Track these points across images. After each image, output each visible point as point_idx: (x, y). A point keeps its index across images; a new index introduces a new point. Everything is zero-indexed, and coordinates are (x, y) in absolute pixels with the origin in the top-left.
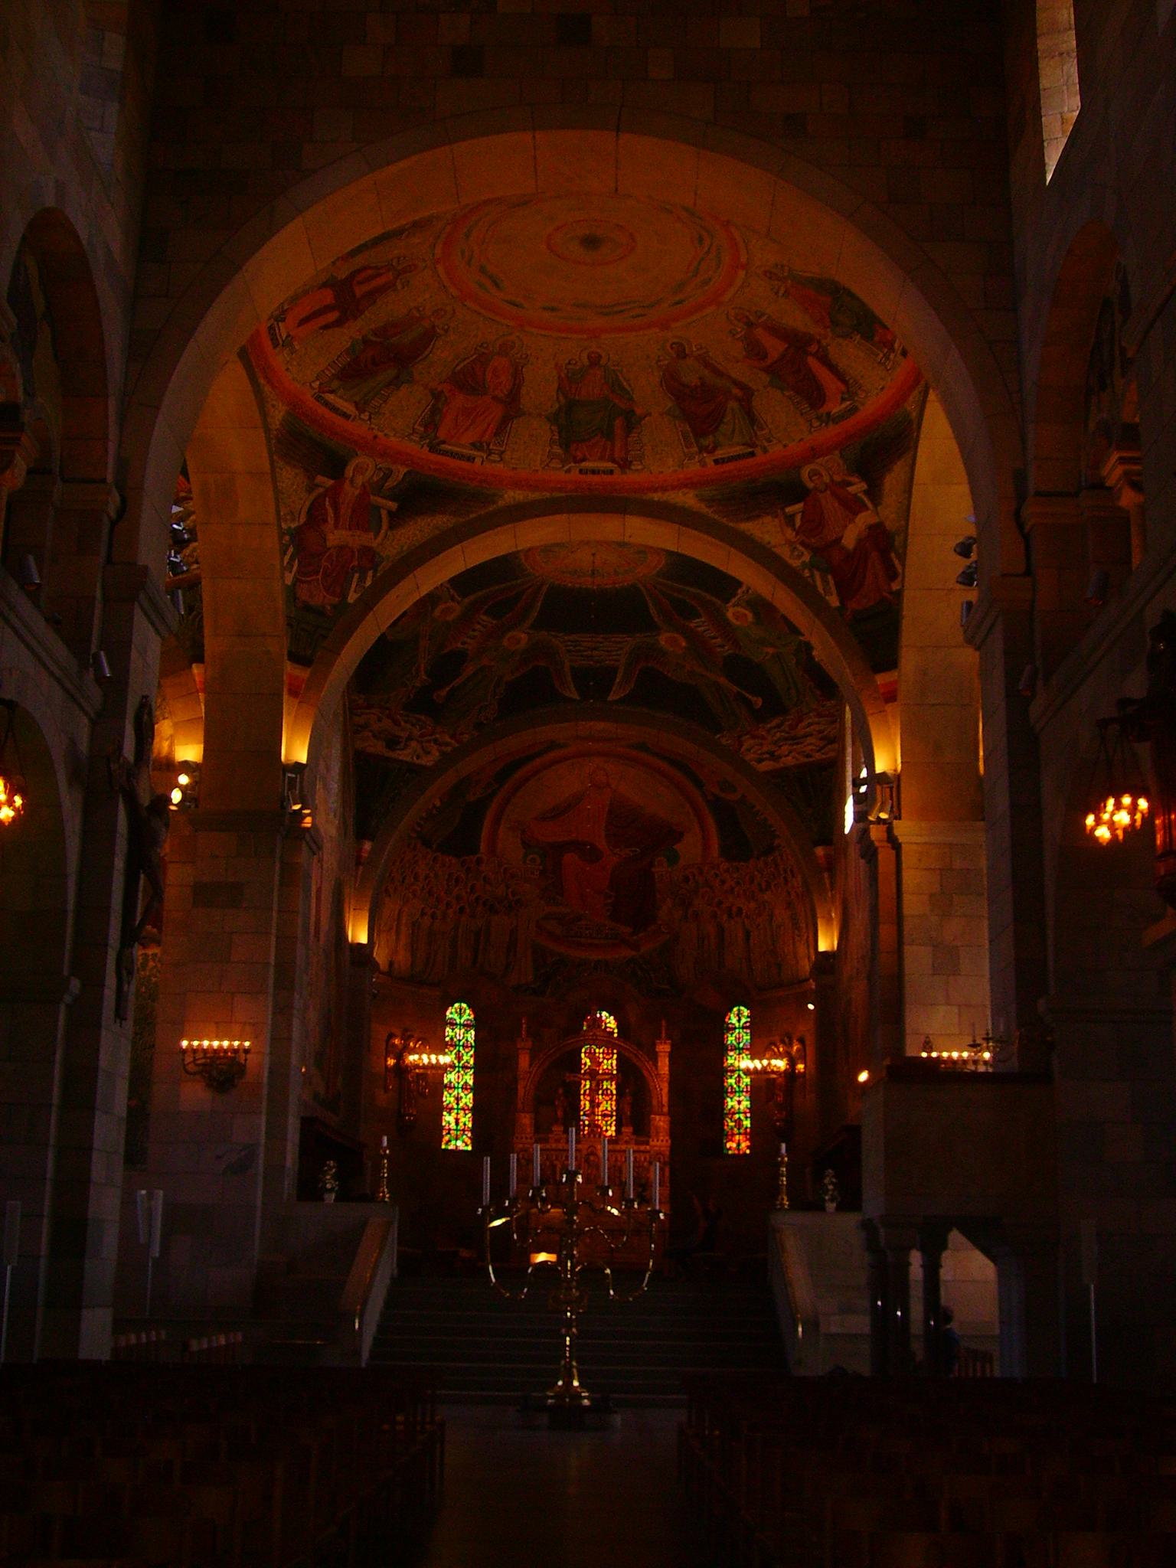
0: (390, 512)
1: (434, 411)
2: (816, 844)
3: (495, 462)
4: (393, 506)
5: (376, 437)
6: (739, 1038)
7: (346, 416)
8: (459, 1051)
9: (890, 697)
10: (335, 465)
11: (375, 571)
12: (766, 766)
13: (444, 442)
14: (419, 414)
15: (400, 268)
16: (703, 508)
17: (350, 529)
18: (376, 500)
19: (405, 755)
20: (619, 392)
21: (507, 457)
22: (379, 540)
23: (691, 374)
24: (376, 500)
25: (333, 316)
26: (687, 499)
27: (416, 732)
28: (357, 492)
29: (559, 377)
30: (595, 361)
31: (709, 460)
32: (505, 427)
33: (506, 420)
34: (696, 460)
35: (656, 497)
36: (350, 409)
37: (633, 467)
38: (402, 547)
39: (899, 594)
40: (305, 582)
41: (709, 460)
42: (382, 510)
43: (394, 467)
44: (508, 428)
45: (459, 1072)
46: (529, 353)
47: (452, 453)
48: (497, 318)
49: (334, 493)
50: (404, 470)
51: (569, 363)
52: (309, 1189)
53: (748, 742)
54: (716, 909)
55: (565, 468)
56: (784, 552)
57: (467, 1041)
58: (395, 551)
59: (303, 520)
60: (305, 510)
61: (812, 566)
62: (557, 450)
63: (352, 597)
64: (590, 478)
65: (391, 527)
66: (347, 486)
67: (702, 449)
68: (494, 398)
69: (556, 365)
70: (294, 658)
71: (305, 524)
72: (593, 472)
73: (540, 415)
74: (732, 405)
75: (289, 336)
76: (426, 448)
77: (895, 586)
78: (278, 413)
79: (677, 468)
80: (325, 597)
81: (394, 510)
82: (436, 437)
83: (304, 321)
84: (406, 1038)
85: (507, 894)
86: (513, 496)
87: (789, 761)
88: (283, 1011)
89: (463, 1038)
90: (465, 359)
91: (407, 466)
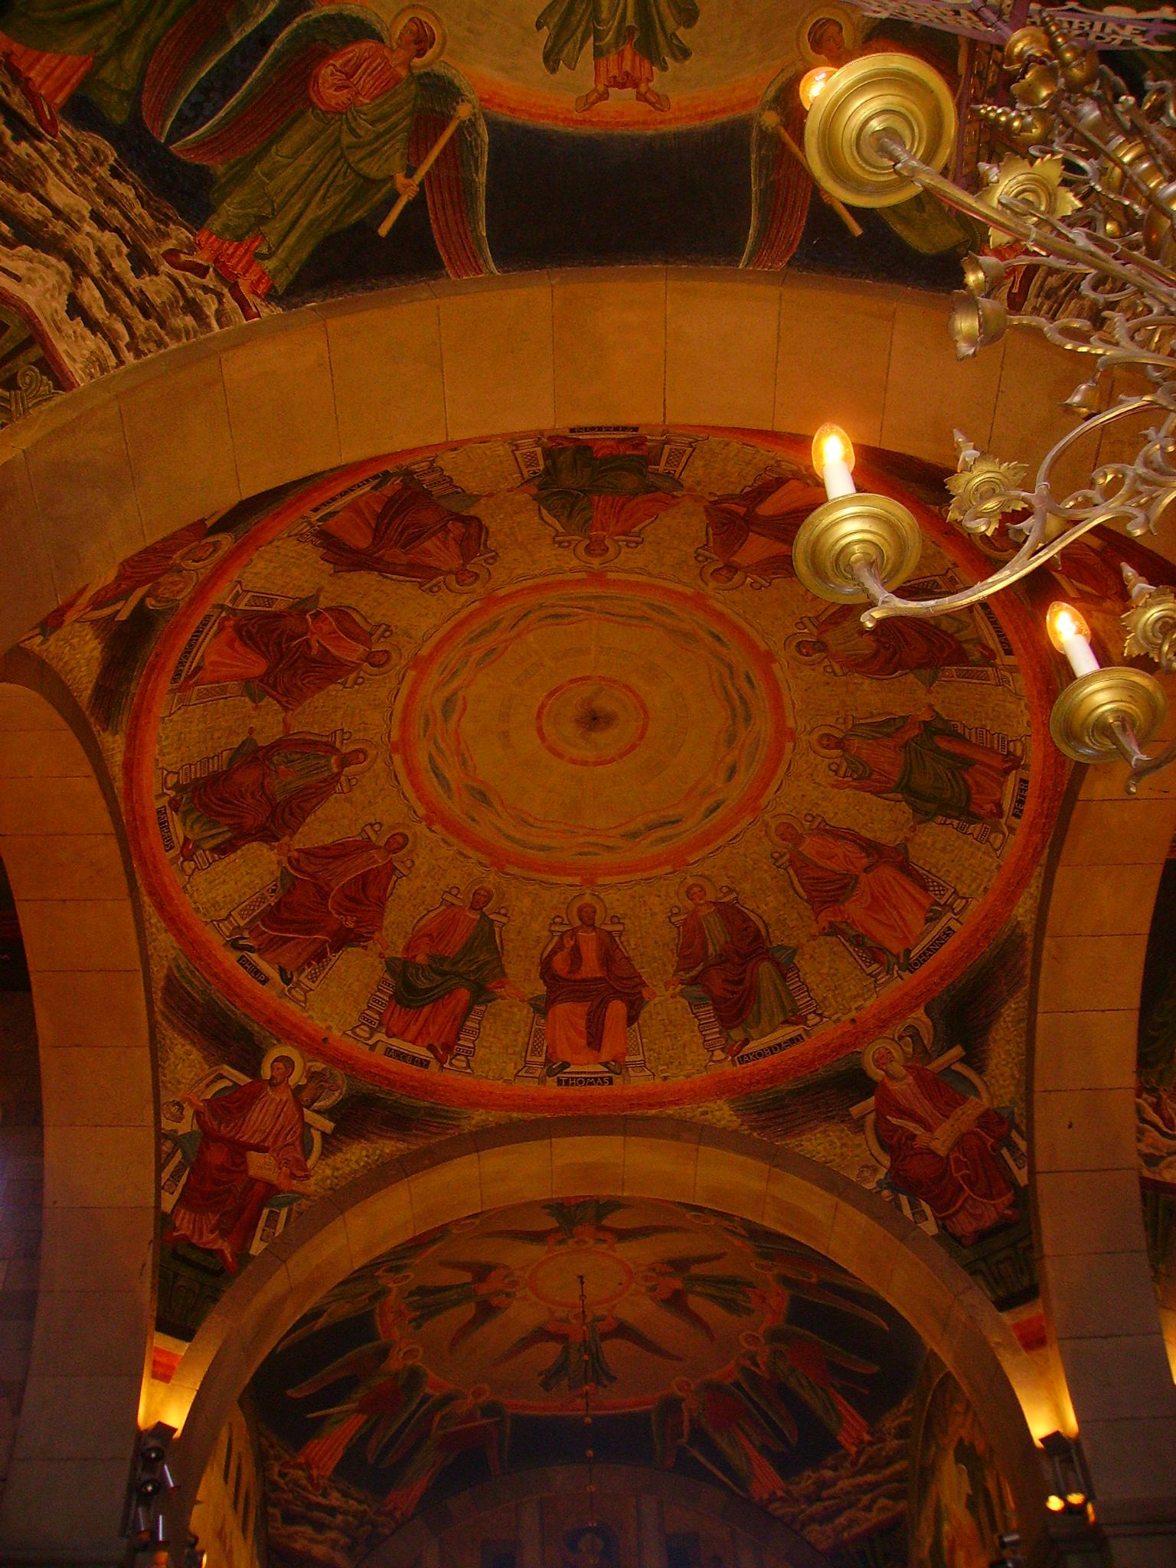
0: (963, 1060)
1: (858, 941)
3: (964, 908)
4: (957, 1051)
5: (853, 1021)
7: (792, 1041)
11: (1017, 1128)
13: (908, 951)
14: (851, 960)
15: (578, 923)
17: (947, 1117)
18: (935, 1066)
20: (893, 729)
21: (963, 890)
22: (985, 1095)
24: (935, 1066)
25: (617, 1009)
28: (910, 1079)
29: (856, 788)
30: (830, 742)
31: (1010, 660)
32: (921, 876)
33: (905, 867)
34: (1007, 674)
36: (791, 1031)
37: (1019, 753)
38: (1013, 1077)
40: (957, 1212)
42: (953, 1067)
43: (909, 1022)
44: (921, 871)
46: (805, 812)
47: (928, 949)
48: (734, 831)
49: (889, 1104)
50: (920, 1012)
51: (836, 772)
55: (1006, 830)
58: (1012, 1088)
59: (886, 1161)
60: (876, 1149)
62: (975, 828)
64: (1030, 806)
65: (980, 1070)
66: (894, 1087)
67: (989, 657)
68: (866, 870)
69: (833, 786)
71: (893, 1161)
72: (1021, 802)
73: (913, 829)
75: (605, 1064)
76: (906, 975)
78: (722, 1113)
79: (1022, 703)
80: (994, 1205)
81: (964, 1053)
82: (897, 957)
83: (595, 1041)
86: (1023, 910)
90: (792, 883)
91: (918, 1006)
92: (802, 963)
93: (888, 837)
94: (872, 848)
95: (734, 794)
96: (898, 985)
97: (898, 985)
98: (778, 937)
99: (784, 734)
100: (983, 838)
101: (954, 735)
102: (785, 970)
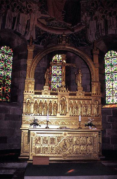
6: (111, 62)
8: (6, 63)
45: (5, 71)
54: (105, 14)
57: (9, 60)
85: (27, 6)
89: (8, 59)
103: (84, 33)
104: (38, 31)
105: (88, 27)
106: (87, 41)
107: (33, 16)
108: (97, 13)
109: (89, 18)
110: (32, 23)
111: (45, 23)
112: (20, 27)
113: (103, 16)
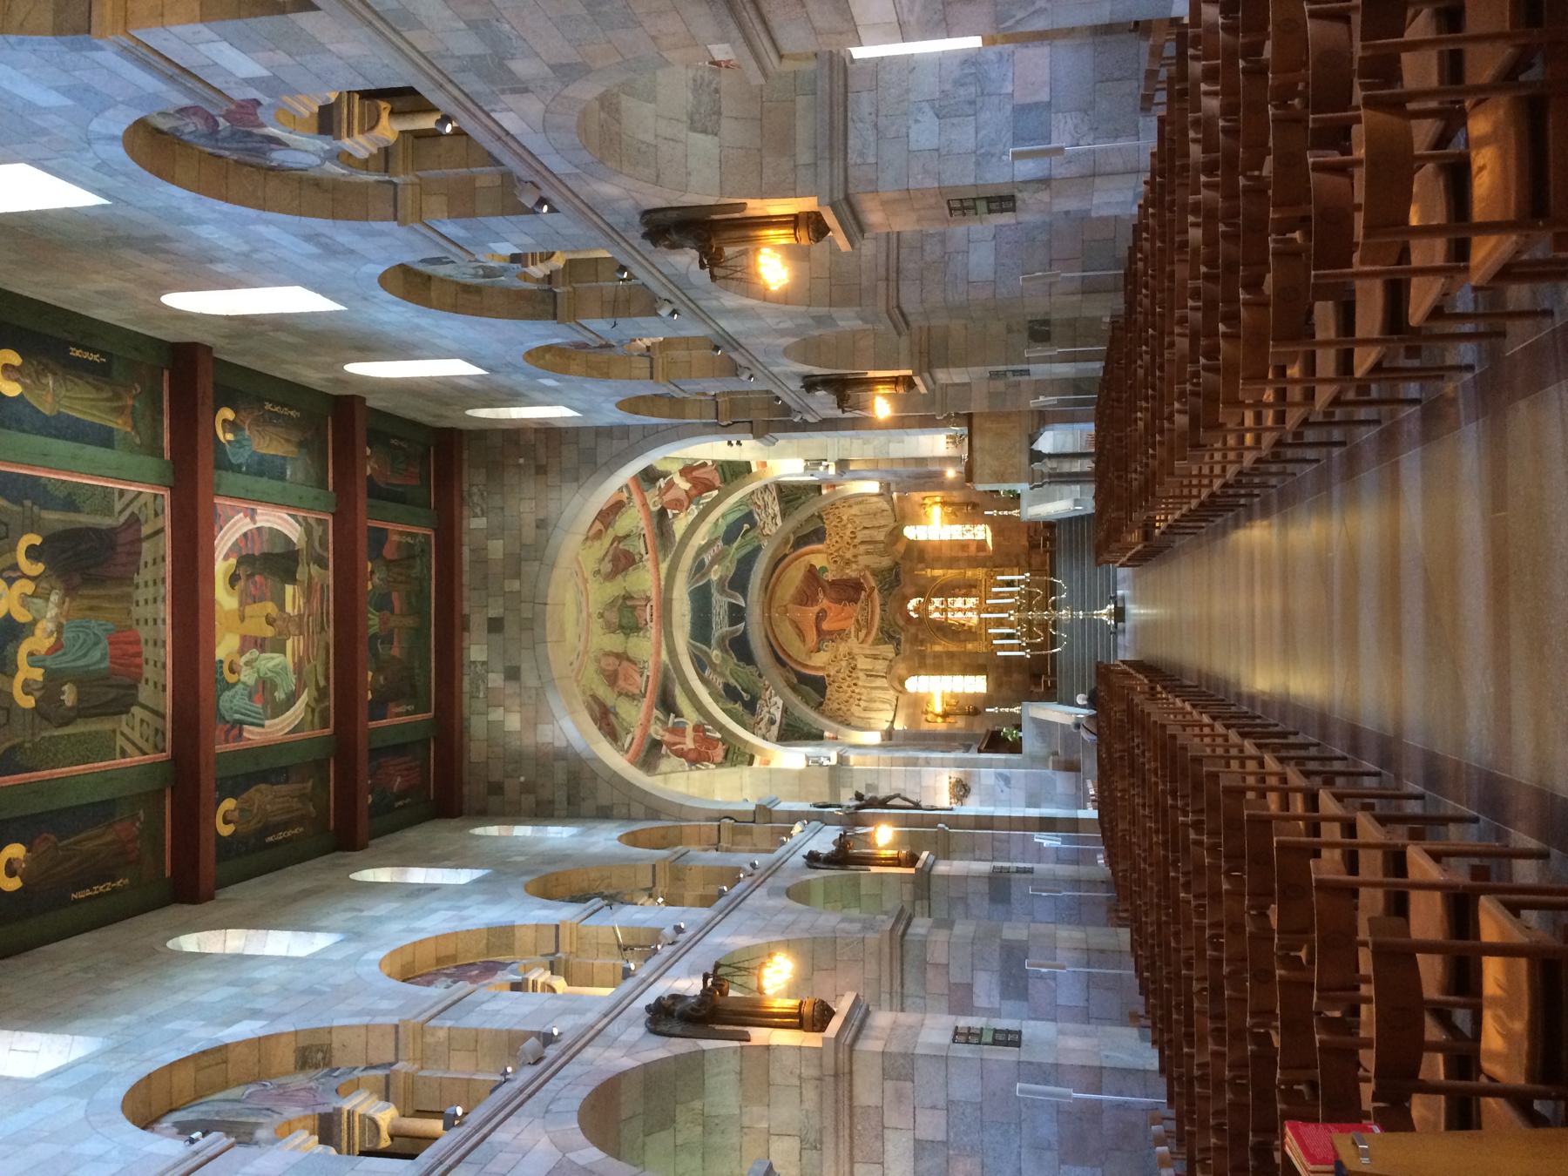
1: (627, 695)
2: (820, 493)
4: (672, 715)
9: (764, 464)
10: (656, 745)
12: (779, 521)
16: (668, 560)
19: (778, 715)
23: (607, 567)
26: (664, 567)
27: (766, 709)
30: (601, 615)
33: (629, 659)
35: (663, 583)
39: (714, 461)
41: (646, 557)
49: (670, 745)
50: (655, 711)
52: (1015, 747)
53: (766, 531)
56: (691, 518)
61: (698, 504)
63: (718, 735)
67: (641, 560)
70: (751, 763)
74: (621, 546)
77: (710, 463)
84: (927, 712)
86: (664, 656)
87: (777, 508)
88: (928, 763)
92: (618, 710)
93: (620, 650)
94: (618, 656)
95: (581, 647)
96: (645, 703)
97: (645, 703)
98: (610, 702)
99: (589, 615)
100: (645, 637)
101: (632, 598)
102: (616, 715)
103: (875, 573)
104: (877, 642)
105: (867, 567)
106: (891, 569)
107: (856, 651)
108: (848, 555)
109: (854, 566)
110: (868, 652)
111: (864, 632)
112: (878, 667)
113: (855, 546)
